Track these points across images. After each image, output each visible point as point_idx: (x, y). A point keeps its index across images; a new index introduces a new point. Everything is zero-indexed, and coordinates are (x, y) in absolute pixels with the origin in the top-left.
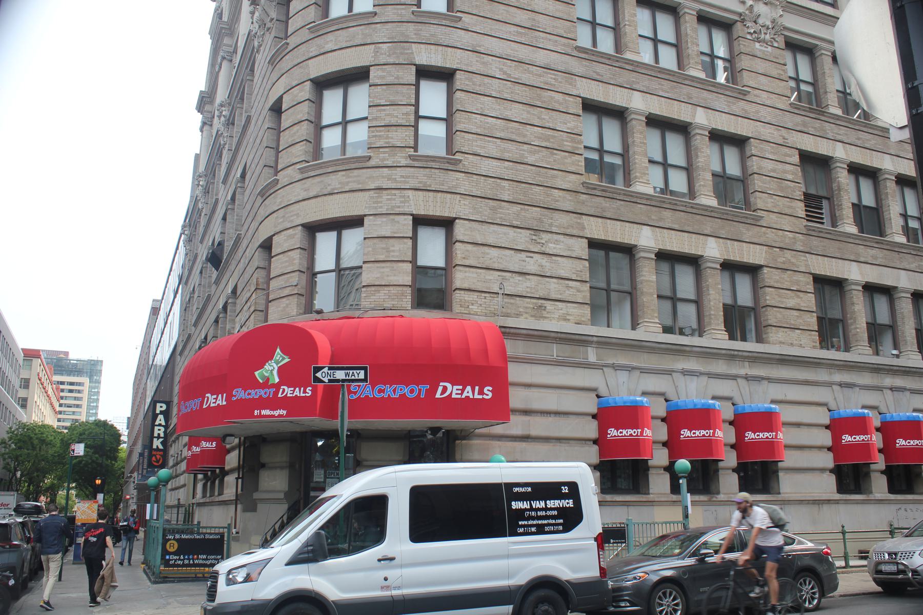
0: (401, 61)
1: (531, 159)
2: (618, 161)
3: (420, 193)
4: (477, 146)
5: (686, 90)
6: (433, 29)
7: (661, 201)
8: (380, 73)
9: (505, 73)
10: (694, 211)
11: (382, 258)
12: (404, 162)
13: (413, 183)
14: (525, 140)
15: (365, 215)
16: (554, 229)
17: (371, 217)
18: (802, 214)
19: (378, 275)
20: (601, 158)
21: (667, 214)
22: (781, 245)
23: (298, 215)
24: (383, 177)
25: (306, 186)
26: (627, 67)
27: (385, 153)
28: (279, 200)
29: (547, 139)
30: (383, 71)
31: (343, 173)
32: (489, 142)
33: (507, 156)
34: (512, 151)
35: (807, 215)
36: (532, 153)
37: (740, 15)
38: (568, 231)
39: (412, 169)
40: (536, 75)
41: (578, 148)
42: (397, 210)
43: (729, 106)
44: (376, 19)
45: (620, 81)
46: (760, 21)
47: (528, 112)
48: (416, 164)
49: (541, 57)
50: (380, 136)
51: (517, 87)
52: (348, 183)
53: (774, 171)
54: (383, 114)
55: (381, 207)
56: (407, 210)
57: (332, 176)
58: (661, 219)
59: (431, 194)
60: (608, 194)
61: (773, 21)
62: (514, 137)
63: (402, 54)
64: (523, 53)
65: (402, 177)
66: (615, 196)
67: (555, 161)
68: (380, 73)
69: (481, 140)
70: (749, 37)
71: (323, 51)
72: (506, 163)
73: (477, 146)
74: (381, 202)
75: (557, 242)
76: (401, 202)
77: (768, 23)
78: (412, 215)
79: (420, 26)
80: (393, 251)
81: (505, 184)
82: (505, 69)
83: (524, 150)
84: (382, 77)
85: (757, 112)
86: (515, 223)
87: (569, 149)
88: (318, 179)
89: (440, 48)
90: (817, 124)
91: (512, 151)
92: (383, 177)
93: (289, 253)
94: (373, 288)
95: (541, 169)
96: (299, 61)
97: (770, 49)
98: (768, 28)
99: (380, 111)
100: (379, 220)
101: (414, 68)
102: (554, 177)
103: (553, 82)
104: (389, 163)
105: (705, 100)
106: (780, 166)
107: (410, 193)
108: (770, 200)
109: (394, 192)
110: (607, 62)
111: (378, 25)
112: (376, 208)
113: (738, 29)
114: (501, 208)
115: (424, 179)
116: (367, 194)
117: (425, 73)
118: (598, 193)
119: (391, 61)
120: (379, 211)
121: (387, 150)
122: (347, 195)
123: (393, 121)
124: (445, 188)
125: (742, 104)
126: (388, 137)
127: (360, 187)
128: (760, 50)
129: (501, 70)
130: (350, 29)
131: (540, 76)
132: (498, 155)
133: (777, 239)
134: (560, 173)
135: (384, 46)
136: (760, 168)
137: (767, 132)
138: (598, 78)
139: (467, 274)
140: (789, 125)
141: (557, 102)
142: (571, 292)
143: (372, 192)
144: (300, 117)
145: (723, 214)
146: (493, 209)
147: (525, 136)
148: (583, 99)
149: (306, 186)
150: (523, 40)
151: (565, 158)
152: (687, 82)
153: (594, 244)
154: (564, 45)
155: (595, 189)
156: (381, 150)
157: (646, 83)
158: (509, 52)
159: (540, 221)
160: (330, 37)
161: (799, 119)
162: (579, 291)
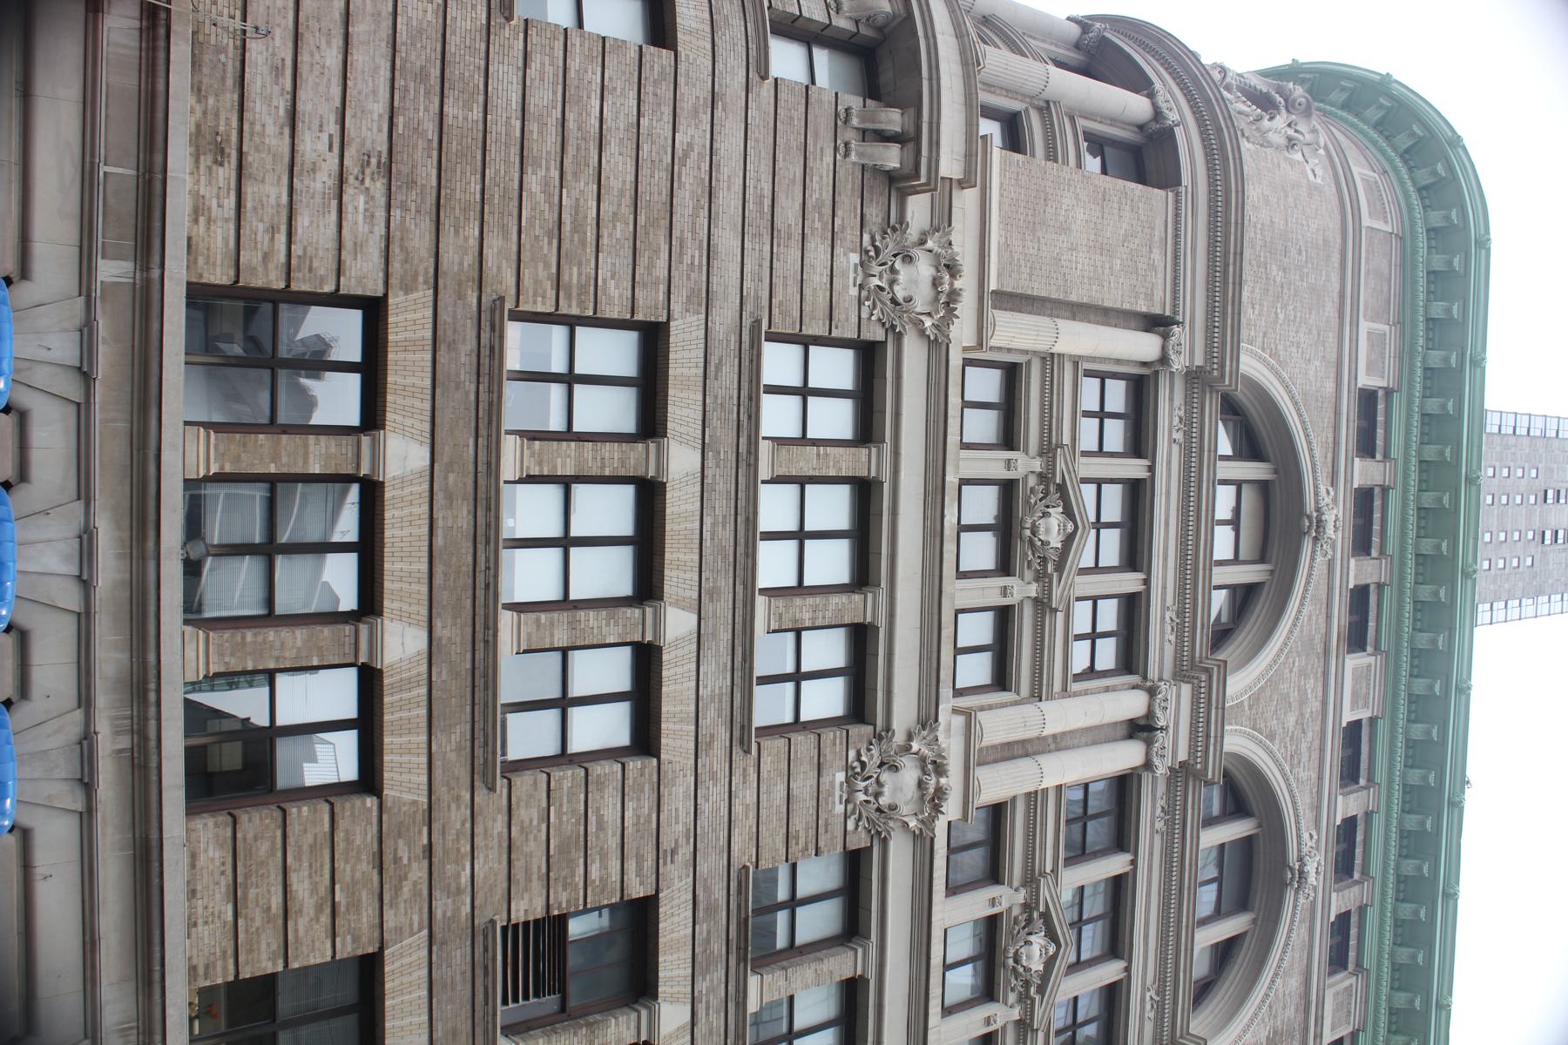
4: (543, 64)
5: (725, 583)
7: (488, 499)
10: (480, 593)
14: (568, 176)
18: (518, 916)
22: (438, 849)
26: (743, 440)
29: (578, 228)
32: (555, 93)
33: (533, 127)
35: (516, 926)
37: (888, 728)
40: (694, 223)
43: (712, 697)
46: (886, 777)
47: (622, 193)
49: (727, 240)
51: (665, 176)
53: (601, 825)
58: (450, 497)
60: (485, 361)
61: (893, 807)
66: (485, 380)
67: (537, 237)
69: (555, 75)
70: (852, 754)
72: (518, 124)
73: (543, 64)
77: (884, 801)
83: (548, 169)
87: (565, 277)
90: (718, 947)
91: (544, 142)
95: (516, 203)
97: (840, 809)
98: (877, 795)
103: (687, 260)
105: (714, 635)
106: (613, 842)
110: (744, 393)
113: (860, 731)
118: (485, 336)
125: (722, 735)
128: (832, 783)
129: (690, 146)
131: (693, 232)
133: (450, 837)
134: (514, 248)
136: (601, 786)
138: (711, 368)
145: (485, 676)
148: (667, 325)
151: (547, 266)
152: (740, 588)
154: (757, 298)
155: (493, 329)
161: (719, 894)
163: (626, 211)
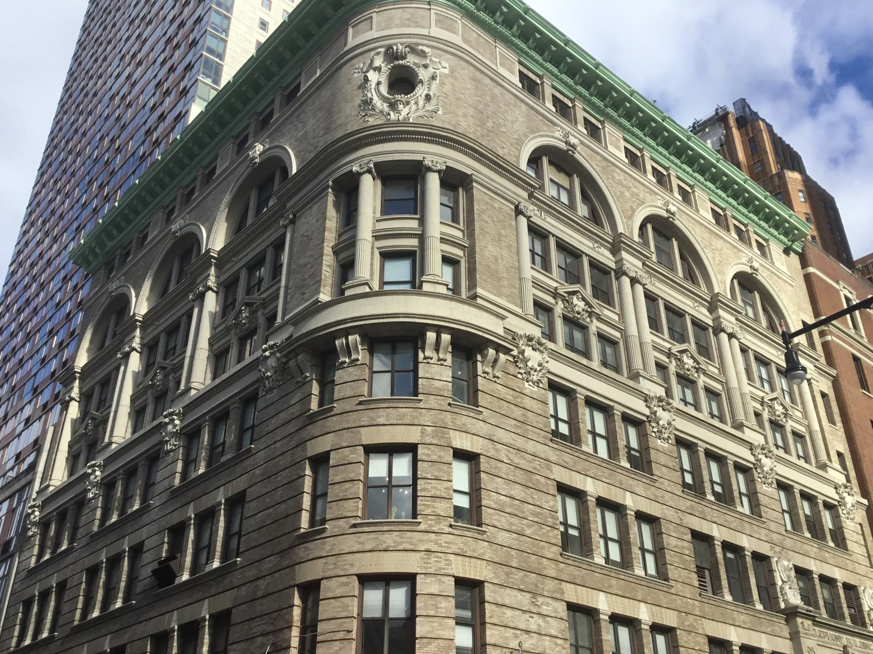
0: (442, 443)
1: (528, 532)
2: (575, 533)
3: (460, 558)
6: (464, 419)
8: (426, 451)
9: (510, 459)
11: (432, 613)
13: (454, 549)
14: (524, 516)
15: (417, 574)
16: (545, 593)
17: (422, 576)
19: (429, 629)
20: (566, 530)
21: (614, 582)
24: (431, 541)
25: (360, 540)
27: (432, 520)
28: (328, 548)
29: (537, 515)
30: (429, 449)
33: (514, 528)
36: (529, 526)
38: (554, 595)
39: (453, 537)
41: (556, 524)
42: (443, 572)
45: (578, 468)
47: (525, 492)
48: (456, 532)
49: (530, 446)
50: (427, 505)
51: (518, 471)
52: (401, 543)
54: (429, 486)
55: (430, 568)
56: (450, 572)
57: (387, 535)
59: (467, 559)
62: (517, 513)
63: (442, 437)
64: (520, 442)
65: (446, 542)
68: (426, 451)
71: (374, 423)
74: (430, 563)
75: (547, 604)
76: (446, 565)
78: (454, 576)
79: (455, 416)
80: (441, 608)
81: (513, 552)
82: (510, 455)
84: (428, 455)
85: (663, 497)
86: (522, 587)
87: (550, 524)
88: (372, 536)
89: (469, 435)
90: (700, 508)
92: (431, 541)
93: (343, 599)
94: (426, 640)
96: (349, 426)
100: (429, 579)
101: (451, 451)
102: (543, 548)
104: (435, 529)
107: (452, 557)
109: (440, 555)
111: (423, 411)
112: (426, 568)
114: (512, 573)
115: (462, 546)
116: (418, 555)
117: (460, 455)
118: (571, 562)
119: (435, 442)
121: (433, 517)
122: (401, 554)
123: (438, 493)
124: (476, 555)
126: (434, 507)
127: (412, 547)
129: (507, 456)
130: (400, 410)
131: (530, 462)
132: (507, 528)
135: (429, 429)
137: (670, 514)
138: (565, 465)
139: (494, 632)
140: (683, 508)
141: (542, 484)
143: (423, 553)
146: (507, 574)
147: (524, 512)
149: (360, 540)
150: (519, 431)
151: (549, 531)
152: (619, 471)
153: (573, 607)
156: (429, 517)
157: (594, 471)
158: (512, 442)
159: (536, 585)
160: (381, 412)
161: (689, 503)
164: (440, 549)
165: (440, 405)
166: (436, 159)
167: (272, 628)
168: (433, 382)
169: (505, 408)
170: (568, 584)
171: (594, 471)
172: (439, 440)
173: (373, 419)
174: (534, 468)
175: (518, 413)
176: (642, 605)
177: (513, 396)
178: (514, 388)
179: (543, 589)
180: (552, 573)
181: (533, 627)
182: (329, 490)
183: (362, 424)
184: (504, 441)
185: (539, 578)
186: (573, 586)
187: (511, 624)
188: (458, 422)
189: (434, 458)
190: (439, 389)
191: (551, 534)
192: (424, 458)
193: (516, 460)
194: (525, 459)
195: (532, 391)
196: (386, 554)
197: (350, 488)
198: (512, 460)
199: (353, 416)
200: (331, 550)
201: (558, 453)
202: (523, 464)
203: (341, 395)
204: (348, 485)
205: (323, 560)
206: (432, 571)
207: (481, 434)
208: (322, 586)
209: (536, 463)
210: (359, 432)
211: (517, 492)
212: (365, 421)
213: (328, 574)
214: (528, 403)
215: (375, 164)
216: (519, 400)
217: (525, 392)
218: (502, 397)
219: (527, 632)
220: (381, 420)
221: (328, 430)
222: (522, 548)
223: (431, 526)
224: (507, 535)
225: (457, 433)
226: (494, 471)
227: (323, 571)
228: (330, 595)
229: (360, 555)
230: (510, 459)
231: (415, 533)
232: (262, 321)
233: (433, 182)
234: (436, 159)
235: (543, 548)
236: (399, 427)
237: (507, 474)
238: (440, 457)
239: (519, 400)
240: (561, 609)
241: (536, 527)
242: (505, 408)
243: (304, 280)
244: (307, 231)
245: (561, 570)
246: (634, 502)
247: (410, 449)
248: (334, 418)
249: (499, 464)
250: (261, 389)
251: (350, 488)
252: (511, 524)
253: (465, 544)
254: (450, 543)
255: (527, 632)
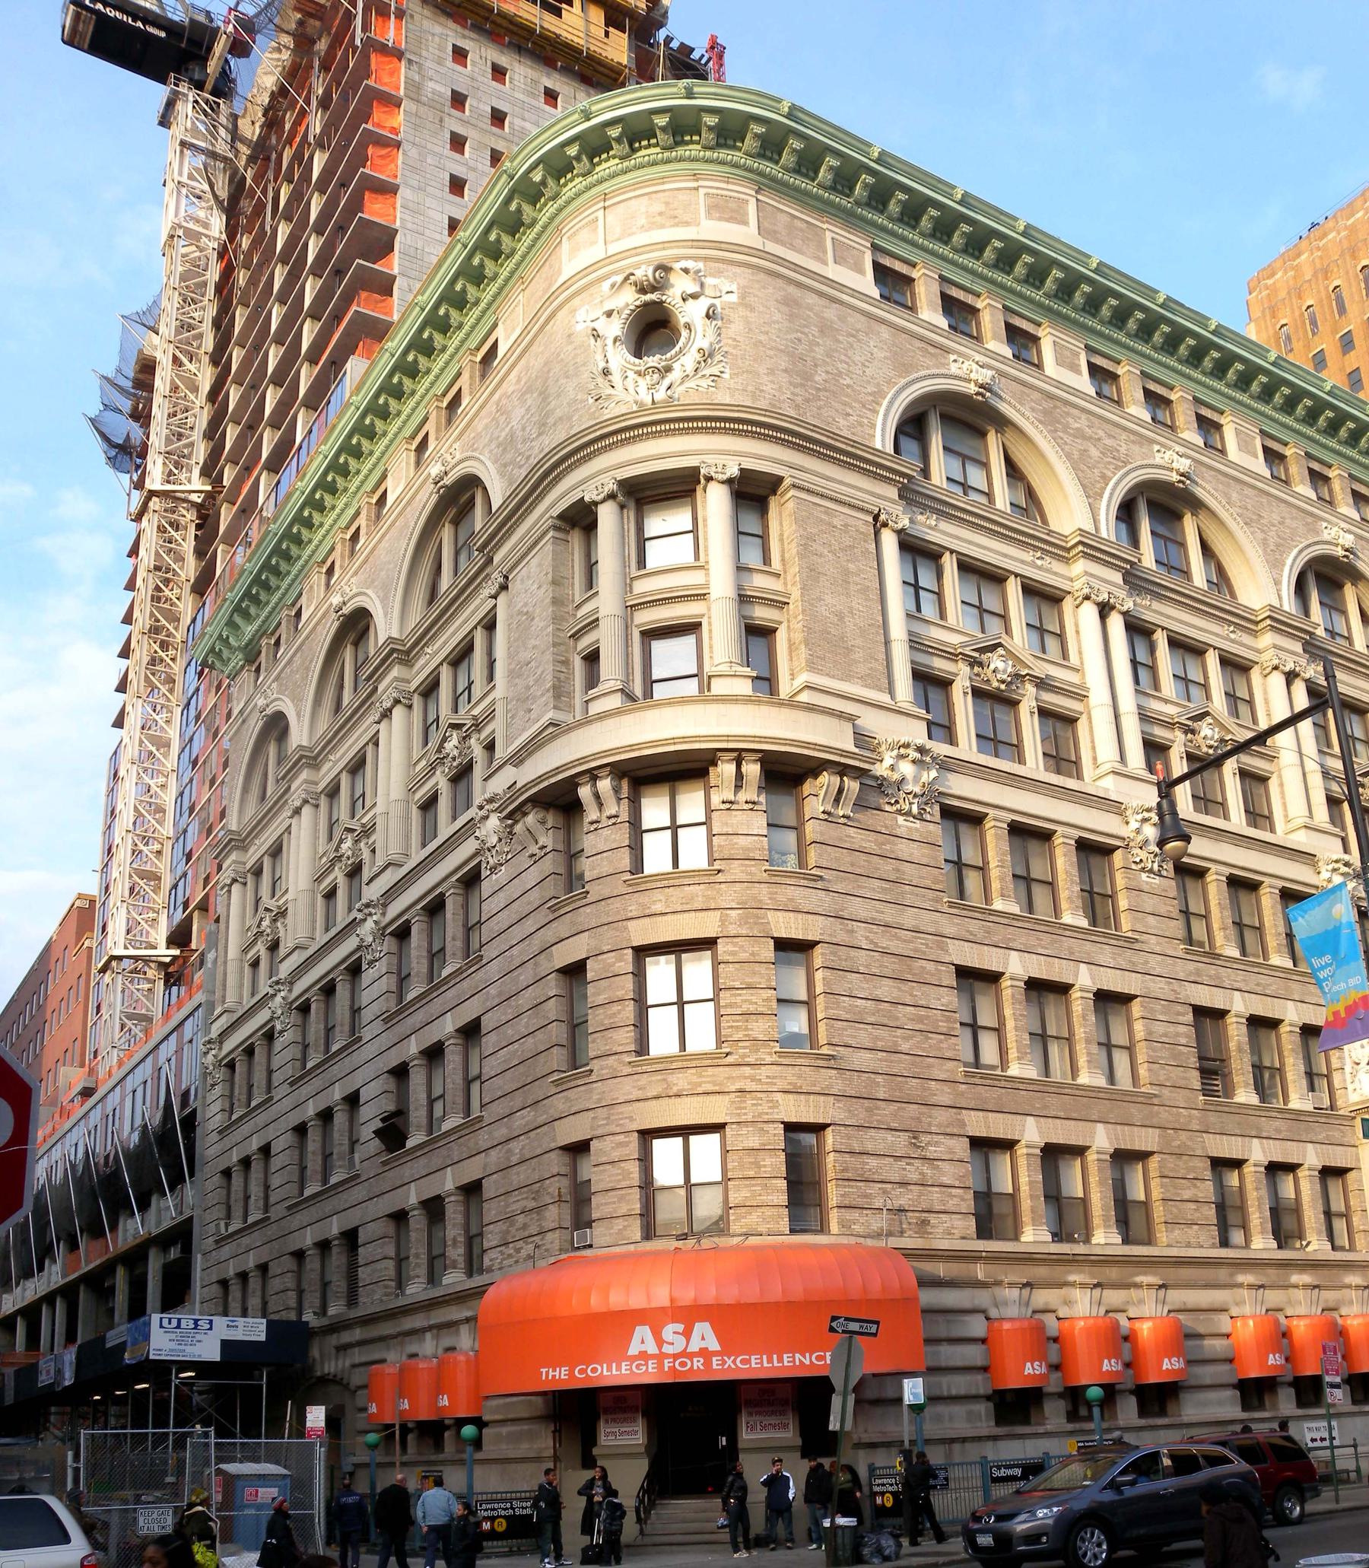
1: (905, 1047)
3: (791, 1096)
5: (1068, 943)
6: (790, 891)
8: (730, 948)
9: (871, 942)
11: (752, 1173)
12: (768, 1059)
14: (898, 1024)
16: (934, 1129)
18: (1197, 1085)
23: (631, 1119)
24: (746, 1078)
27: (744, 1048)
29: (920, 1019)
30: (735, 944)
31: (693, 1071)
33: (880, 1044)
34: (884, 1037)
36: (906, 1038)
38: (948, 1131)
39: (780, 1068)
42: (766, 1118)
44: (720, 877)
45: (995, 939)
47: (899, 989)
49: (909, 918)
51: (886, 958)
53: (1165, 1035)
59: (803, 1097)
62: (885, 1021)
64: (889, 914)
68: (730, 948)
70: (1134, 866)
71: (647, 912)
75: (937, 1144)
79: (774, 888)
81: (879, 1079)
84: (733, 953)
87: (944, 1030)
89: (800, 916)
91: (884, 1037)
92: (746, 1078)
93: (623, 1165)
96: (610, 919)
99: (735, 995)
102: (929, 1066)
104: (751, 1060)
106: (1172, 1028)
107: (779, 1097)
108: (1162, 1072)
109: (759, 1095)
111: (723, 886)
114: (878, 1108)
115: (794, 1080)
116: (727, 1098)
119: (744, 932)
120: (743, 1118)
121: (747, 1044)
122: (700, 1098)
123: (752, 1008)
124: (817, 1089)
126: (747, 1029)
127: (717, 1089)
129: (867, 938)
130: (687, 888)
138: (971, 938)
142: (955, 1201)
144: (620, 994)
146: (869, 1110)
147: (897, 1019)
150: (888, 898)
151: (941, 1041)
157: (1023, 940)
160: (658, 895)
162: (963, 1200)
163: (906, 987)
164: (759, 1088)
165: (751, 874)
166: (720, 460)
167: (533, 1204)
168: (735, 839)
169: (862, 863)
170: (972, 1113)
171: (1023, 940)
172: (751, 929)
173: (643, 906)
174: (916, 950)
175: (887, 868)
176: (1100, 1126)
177: (876, 842)
178: (879, 829)
179: (930, 1124)
180: (946, 1100)
181: (914, 1177)
182: (590, 1017)
183: (630, 915)
184: (863, 915)
185: (924, 1109)
186: (981, 1114)
187: (876, 1177)
188: (779, 897)
189: (743, 956)
190: (748, 849)
191: (944, 1045)
192: (727, 958)
193: (885, 943)
194: (899, 939)
195: (910, 829)
196: (678, 1100)
197: (619, 1012)
198: (876, 944)
199: (616, 904)
200: (599, 1100)
201: (957, 920)
202: (894, 946)
203: (595, 874)
204: (616, 1008)
205: (591, 1114)
206: (749, 1118)
207: (820, 910)
208: (592, 1148)
209: (920, 943)
210: (626, 928)
211: (886, 990)
212: (633, 910)
213: (599, 1132)
214: (904, 849)
215: (622, 483)
216: (888, 847)
217: (898, 832)
218: (857, 847)
219: (903, 1184)
220: (658, 907)
221: (581, 928)
222: (895, 1071)
223: (744, 1056)
224: (868, 1055)
225: (779, 913)
226: (844, 965)
227: (592, 1128)
228: (604, 1159)
229: (641, 1104)
230: (871, 942)
231: (721, 1069)
232: (478, 752)
233: (716, 501)
234: (720, 460)
235: (929, 1066)
236: (686, 915)
237: (866, 967)
238: (753, 954)
239: (888, 847)
240: (962, 1148)
241: (919, 1037)
242: (862, 863)
243: (528, 688)
244: (526, 605)
245: (962, 1094)
246: (1092, 978)
247: (707, 944)
248: (588, 910)
249: (853, 953)
250: (484, 865)
251: (619, 1012)
252: (877, 1038)
253: (800, 1077)
254: (774, 1077)
255: (903, 1184)
